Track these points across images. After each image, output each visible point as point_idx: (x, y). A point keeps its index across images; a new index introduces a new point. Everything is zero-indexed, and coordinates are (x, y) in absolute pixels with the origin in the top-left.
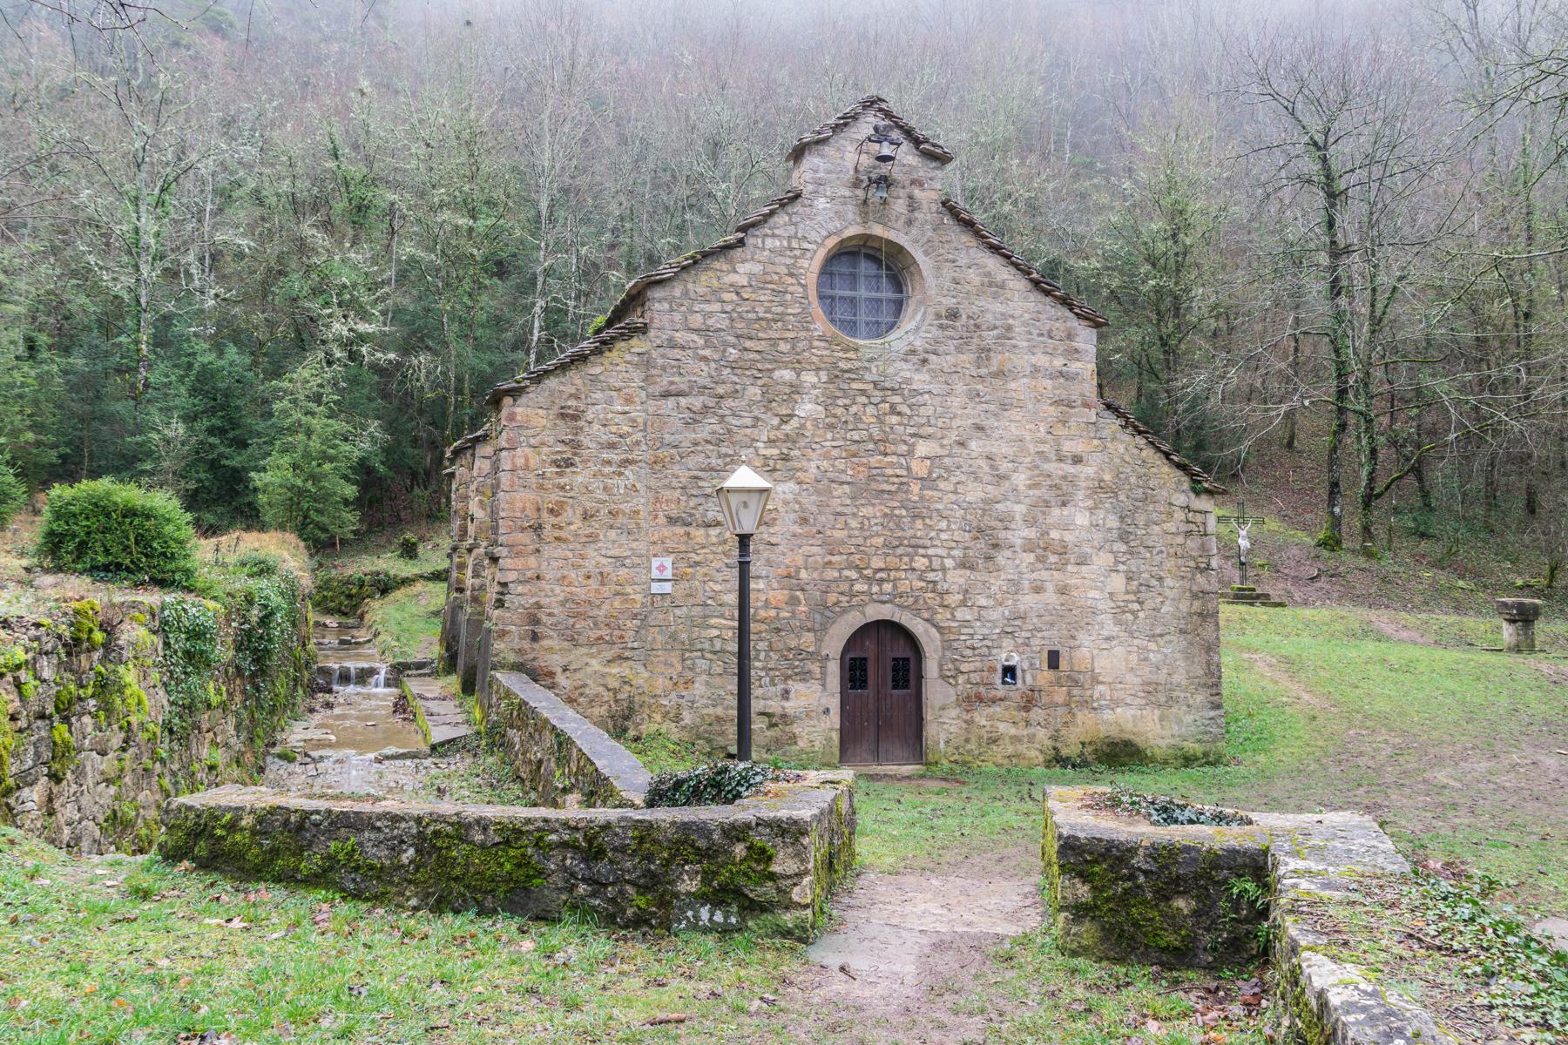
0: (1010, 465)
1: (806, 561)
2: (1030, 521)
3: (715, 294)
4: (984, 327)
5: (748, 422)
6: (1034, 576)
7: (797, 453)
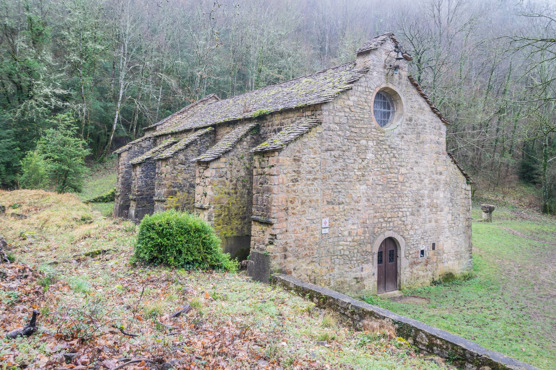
0: (424, 176)
1: (369, 216)
2: (429, 197)
3: (342, 110)
4: (419, 125)
5: (352, 161)
6: (429, 216)
7: (366, 173)
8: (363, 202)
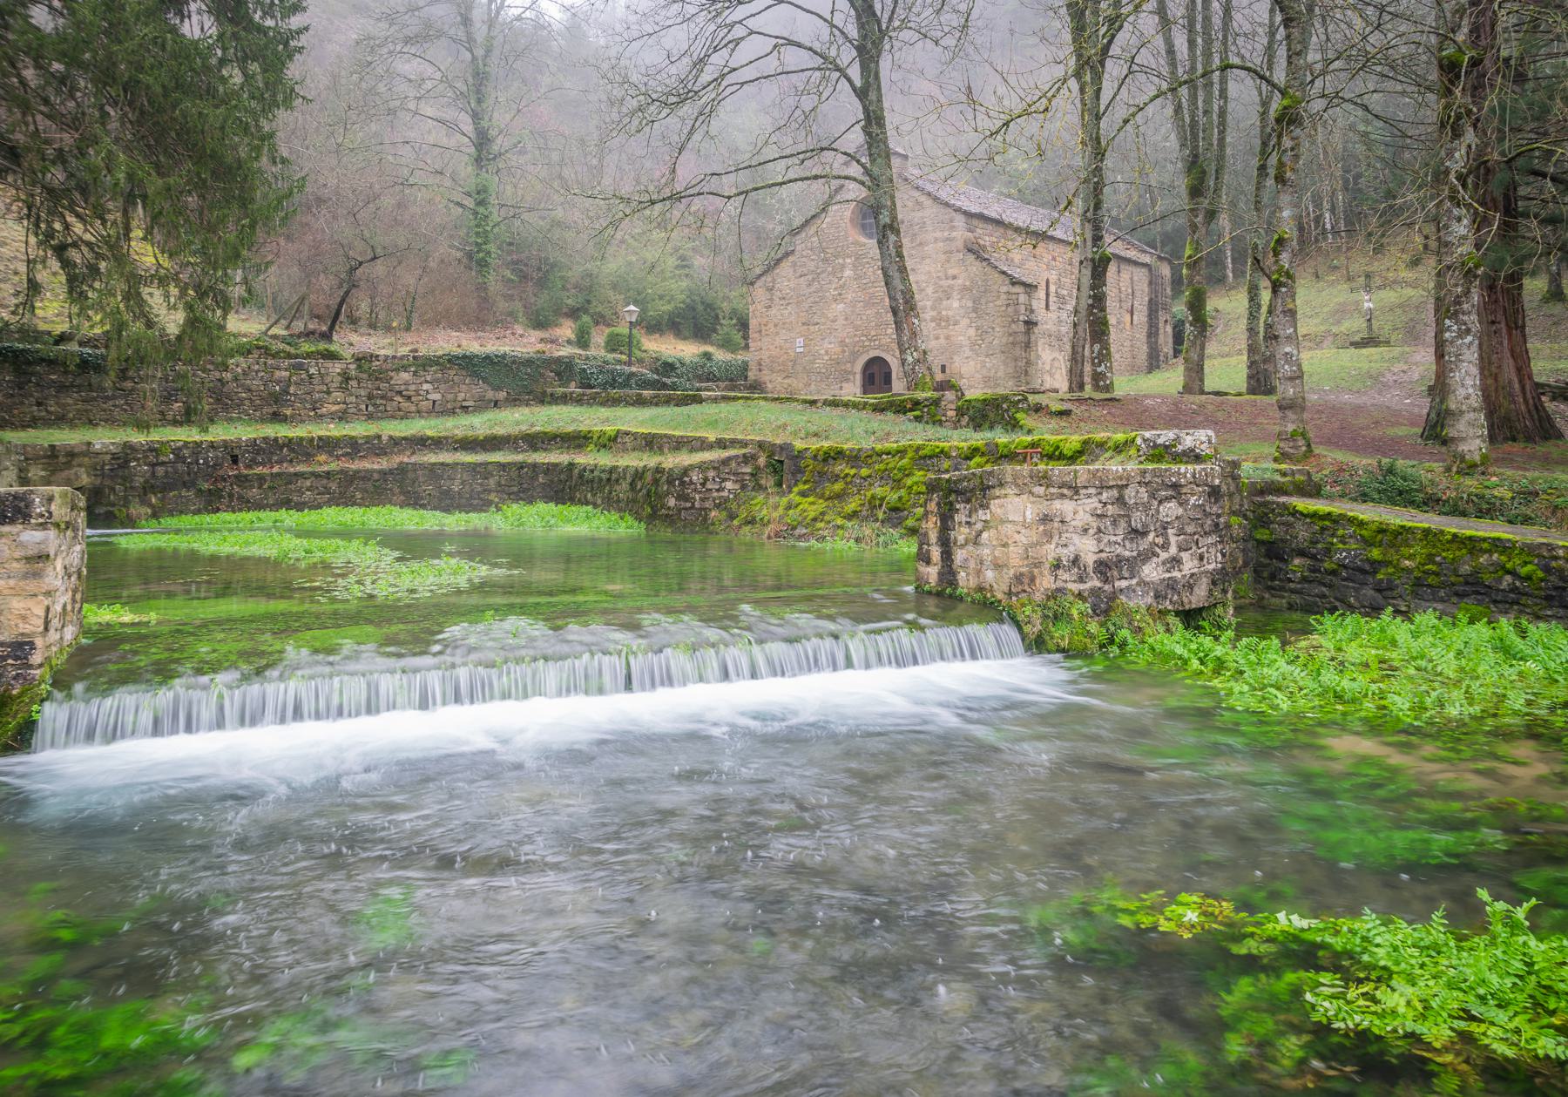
2: (933, 308)
8: (841, 321)
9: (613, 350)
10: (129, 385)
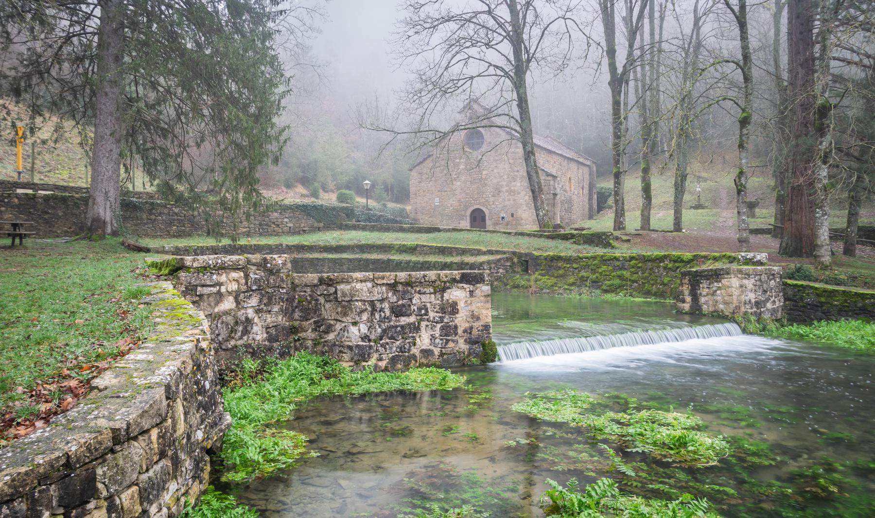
2: (507, 186)
8: (459, 190)
9: (342, 202)
10: (153, 217)
